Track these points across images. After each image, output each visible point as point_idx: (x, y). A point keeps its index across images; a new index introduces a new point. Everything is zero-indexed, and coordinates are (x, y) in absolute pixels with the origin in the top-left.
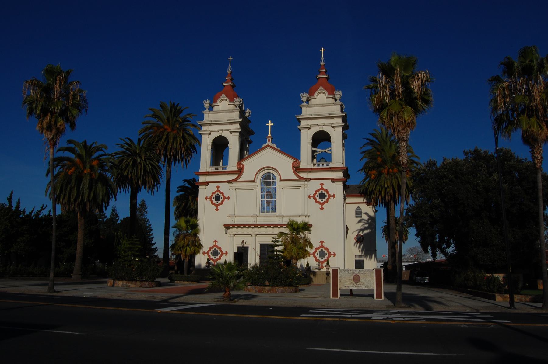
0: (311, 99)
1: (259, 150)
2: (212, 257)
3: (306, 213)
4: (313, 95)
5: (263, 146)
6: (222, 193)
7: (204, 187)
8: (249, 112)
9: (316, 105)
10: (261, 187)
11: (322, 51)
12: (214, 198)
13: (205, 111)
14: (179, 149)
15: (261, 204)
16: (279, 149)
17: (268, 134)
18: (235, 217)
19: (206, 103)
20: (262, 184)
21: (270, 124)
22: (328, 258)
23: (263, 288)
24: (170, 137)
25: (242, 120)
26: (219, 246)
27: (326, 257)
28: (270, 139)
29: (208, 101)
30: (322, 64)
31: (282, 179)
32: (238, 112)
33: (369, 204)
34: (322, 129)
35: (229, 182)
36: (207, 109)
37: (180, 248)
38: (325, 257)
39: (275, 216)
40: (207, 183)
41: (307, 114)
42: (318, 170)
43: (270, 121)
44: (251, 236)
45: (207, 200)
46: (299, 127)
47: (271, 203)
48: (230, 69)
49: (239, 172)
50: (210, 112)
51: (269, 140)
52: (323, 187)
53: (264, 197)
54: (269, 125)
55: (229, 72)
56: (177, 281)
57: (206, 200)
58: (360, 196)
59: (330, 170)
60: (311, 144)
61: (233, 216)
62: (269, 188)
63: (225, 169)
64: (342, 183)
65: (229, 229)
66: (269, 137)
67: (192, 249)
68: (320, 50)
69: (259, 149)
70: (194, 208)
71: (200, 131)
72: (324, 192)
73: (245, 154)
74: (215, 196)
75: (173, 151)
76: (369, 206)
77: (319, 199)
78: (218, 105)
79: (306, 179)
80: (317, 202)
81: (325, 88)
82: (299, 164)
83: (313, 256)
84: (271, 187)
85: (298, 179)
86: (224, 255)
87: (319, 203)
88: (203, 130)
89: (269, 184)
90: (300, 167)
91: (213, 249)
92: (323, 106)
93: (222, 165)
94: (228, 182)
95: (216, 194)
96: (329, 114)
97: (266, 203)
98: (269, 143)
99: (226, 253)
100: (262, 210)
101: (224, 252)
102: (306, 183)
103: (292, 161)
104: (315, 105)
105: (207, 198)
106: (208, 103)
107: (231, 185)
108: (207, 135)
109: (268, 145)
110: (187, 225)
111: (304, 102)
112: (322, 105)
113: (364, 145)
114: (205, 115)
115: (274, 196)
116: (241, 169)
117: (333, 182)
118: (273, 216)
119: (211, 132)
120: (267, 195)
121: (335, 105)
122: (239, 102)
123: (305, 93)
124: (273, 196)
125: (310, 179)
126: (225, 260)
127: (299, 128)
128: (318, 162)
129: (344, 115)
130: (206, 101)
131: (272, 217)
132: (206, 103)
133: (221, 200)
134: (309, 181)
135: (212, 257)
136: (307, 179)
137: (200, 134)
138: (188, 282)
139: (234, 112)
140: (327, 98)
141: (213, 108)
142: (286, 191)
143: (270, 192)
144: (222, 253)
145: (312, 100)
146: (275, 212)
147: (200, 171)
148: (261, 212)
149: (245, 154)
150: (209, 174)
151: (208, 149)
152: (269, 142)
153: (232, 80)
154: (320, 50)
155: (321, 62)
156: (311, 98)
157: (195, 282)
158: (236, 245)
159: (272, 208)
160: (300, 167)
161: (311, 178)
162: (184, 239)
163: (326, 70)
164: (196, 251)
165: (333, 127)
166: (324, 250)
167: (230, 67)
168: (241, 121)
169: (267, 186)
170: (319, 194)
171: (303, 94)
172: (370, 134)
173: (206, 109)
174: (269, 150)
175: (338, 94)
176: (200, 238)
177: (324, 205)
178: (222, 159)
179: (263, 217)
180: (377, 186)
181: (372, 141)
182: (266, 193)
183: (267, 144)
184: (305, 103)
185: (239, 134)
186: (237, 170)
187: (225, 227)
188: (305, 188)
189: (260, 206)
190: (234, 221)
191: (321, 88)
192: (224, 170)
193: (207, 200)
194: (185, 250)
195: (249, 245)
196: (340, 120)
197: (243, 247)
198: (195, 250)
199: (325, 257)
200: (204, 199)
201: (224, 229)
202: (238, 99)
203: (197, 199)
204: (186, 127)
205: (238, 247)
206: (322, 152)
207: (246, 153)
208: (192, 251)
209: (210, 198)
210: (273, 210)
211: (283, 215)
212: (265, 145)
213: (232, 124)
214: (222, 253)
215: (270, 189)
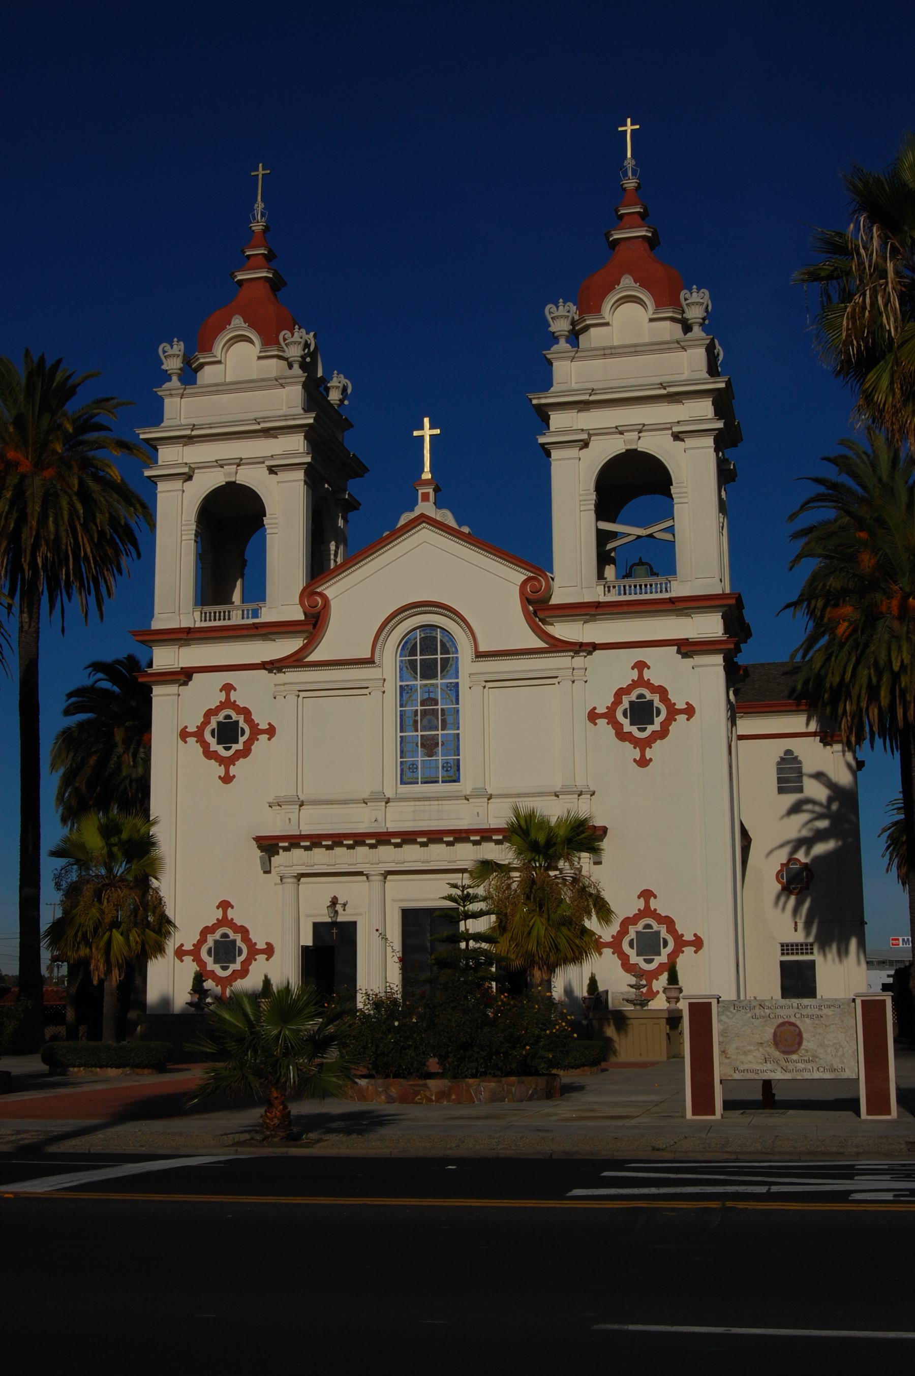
0: (587, 328)
1: (388, 537)
2: (211, 965)
3: (580, 783)
4: (598, 310)
5: (402, 521)
6: (246, 712)
7: (173, 689)
8: (341, 385)
10: (399, 684)
11: (626, 131)
12: (213, 730)
13: (167, 385)
14: (67, 541)
15: (402, 752)
16: (466, 530)
17: (422, 470)
18: (301, 806)
19: (170, 356)
20: (401, 670)
21: (427, 432)
22: (673, 956)
23: (418, 1085)
24: (28, 493)
25: (315, 419)
26: (239, 922)
27: (665, 952)
28: (431, 491)
29: (178, 348)
30: (630, 183)
31: (482, 648)
32: (300, 387)
33: (832, 736)
34: (634, 447)
35: (272, 666)
36: (175, 378)
37: (84, 936)
38: (659, 954)
39: (457, 798)
40: (185, 676)
41: (574, 386)
42: (625, 609)
43: (426, 421)
44: (365, 878)
45: (186, 742)
46: (542, 440)
47: (442, 745)
48: (263, 215)
49: (310, 628)
50: (187, 391)
51: (426, 497)
52: (647, 674)
53: (411, 723)
54: (423, 436)
55: (257, 227)
56: (74, 1067)
57: (181, 742)
58: (794, 708)
59: (670, 607)
60: (593, 507)
61: (290, 803)
62: (432, 685)
63: (253, 617)
64: (719, 659)
65: (278, 854)
66: (426, 483)
67: (131, 938)
68: (620, 129)
69: (387, 533)
70: (134, 776)
71: (149, 467)
72: (649, 696)
73: (332, 552)
74: (219, 723)
75: (44, 548)
76: (831, 745)
78: (219, 362)
79: (577, 648)
80: (622, 736)
81: (644, 283)
82: (549, 589)
83: (613, 953)
84: (439, 681)
85: (545, 645)
86: (261, 958)
87: (630, 742)
88: (160, 463)
89: (429, 670)
90: (554, 601)
91: (217, 935)
92: (636, 353)
93: (243, 601)
94: (267, 666)
95: (221, 717)
96: (661, 384)
97: (423, 746)
98: (426, 508)
99: (269, 951)
100: (407, 775)
101: (261, 945)
102: (579, 661)
103: (518, 576)
104: (604, 349)
105: (184, 735)
106: (178, 356)
107: (280, 678)
108: (177, 484)
109: (422, 516)
110: (110, 845)
111: (562, 341)
112: (633, 349)
113: (803, 507)
114: (167, 401)
115: (451, 719)
116: (320, 612)
117: (685, 656)
118: (451, 798)
119: (192, 470)
120: (424, 713)
121: (684, 349)
122: (301, 347)
123: (565, 303)
124: (450, 719)
125: (594, 647)
126: (266, 977)
127: (543, 445)
128: (624, 577)
129: (723, 385)
130: (168, 347)
131: (444, 802)
132: (170, 356)
133: (242, 740)
134: (590, 653)
135: (211, 965)
136: (581, 645)
137: (149, 477)
138: (120, 1070)
139: (282, 386)
140: (651, 320)
141: (199, 374)
142: (495, 695)
143: (437, 704)
144: (253, 952)
145: (592, 330)
146: (457, 780)
147: (157, 624)
148: (402, 783)
149: (332, 552)
150: (190, 636)
151: (184, 538)
152: (426, 503)
153: (269, 258)
154: (620, 129)
155: (625, 174)
156: (588, 322)
157: (146, 1071)
158: (308, 916)
159: (446, 767)
160: (554, 601)
161: (598, 641)
162: (100, 901)
163: (645, 209)
164: (147, 947)
165: (677, 437)
166: (655, 926)
167: (259, 206)
168: (311, 421)
169: (423, 677)
170: (631, 703)
171: (554, 308)
172: (829, 460)
173: (170, 380)
174: (425, 534)
175: (697, 303)
176: (162, 894)
177: (651, 748)
178: (242, 576)
179: (412, 803)
180: (860, 668)
181: (834, 486)
182: (419, 708)
183: (417, 512)
184: (563, 345)
185: (306, 473)
186: (302, 617)
187: (259, 847)
188: (573, 682)
189: (399, 760)
190: (294, 818)
191: (627, 281)
192: (251, 621)
193: (186, 742)
194: (102, 944)
195: (361, 914)
196: (705, 408)
197: (334, 924)
198: (143, 944)
199: (659, 954)
200: (175, 735)
201: (258, 853)
202: (296, 334)
203: (145, 737)
204: (91, 454)
205: (316, 926)
206: (639, 537)
207: (337, 547)
208: (133, 944)
209: (199, 735)
210: (452, 773)
211: (489, 792)
212: (412, 515)
213: (276, 437)
214: (253, 952)
215: (436, 692)
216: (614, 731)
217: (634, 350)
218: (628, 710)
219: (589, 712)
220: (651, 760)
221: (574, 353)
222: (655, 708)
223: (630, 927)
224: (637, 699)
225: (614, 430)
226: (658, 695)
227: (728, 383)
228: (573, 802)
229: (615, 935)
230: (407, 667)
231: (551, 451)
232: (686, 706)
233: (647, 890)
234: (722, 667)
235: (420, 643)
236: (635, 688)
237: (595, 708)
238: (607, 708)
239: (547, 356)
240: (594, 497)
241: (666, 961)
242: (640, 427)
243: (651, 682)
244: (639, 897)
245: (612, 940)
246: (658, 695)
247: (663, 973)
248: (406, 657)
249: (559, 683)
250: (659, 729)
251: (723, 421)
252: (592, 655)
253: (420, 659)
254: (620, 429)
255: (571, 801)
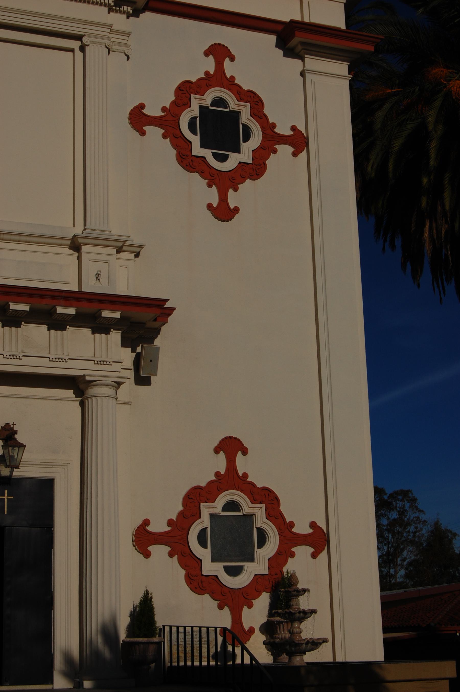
77: (203, 145)
83: (171, 555)
87: (202, 174)
134: (136, 13)
170: (202, 109)
177: (236, 190)
199: (252, 559)
216: (174, 152)
218: (198, 119)
219: (132, 110)
220: (236, 210)
222: (241, 126)
223: (202, 504)
224: (212, 105)
226: (248, 105)
228: (106, 262)
229: (174, 519)
232: (291, 133)
233: (231, 437)
234: (348, 82)
236: (209, 87)
237: (142, 106)
238: (164, 109)
241: (266, 572)
243: (236, 82)
244: (217, 451)
245: (169, 529)
246: (248, 105)
247: (260, 594)
249: (82, 49)
250: (251, 162)
252: (138, 17)
255: (105, 258)
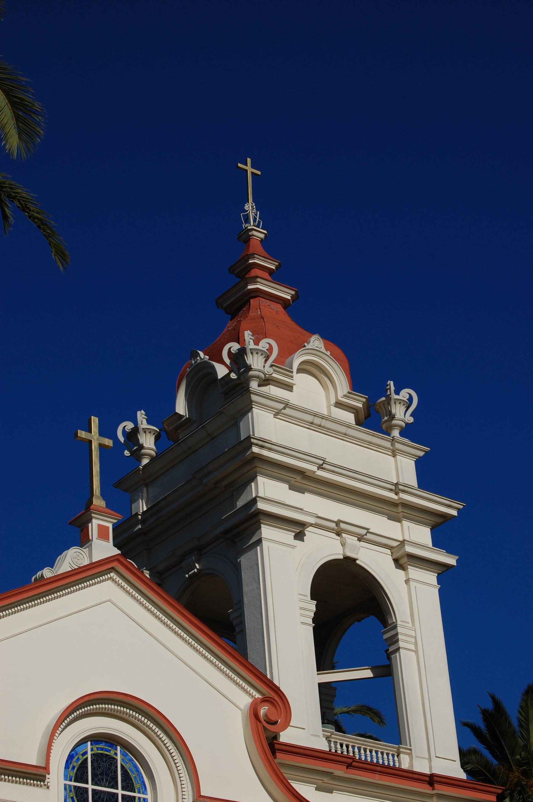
9: (317, 421)
28: (110, 526)
60: (310, 621)
129: (454, 513)
217: (344, 431)
221: (283, 405)
225: (333, 525)
227: (459, 510)
230: (72, 798)
231: (262, 525)
235: (92, 762)
239: (252, 395)
240: (312, 606)
242: (364, 532)
248: (71, 780)
251: (457, 557)
253: (87, 789)
254: (342, 526)
